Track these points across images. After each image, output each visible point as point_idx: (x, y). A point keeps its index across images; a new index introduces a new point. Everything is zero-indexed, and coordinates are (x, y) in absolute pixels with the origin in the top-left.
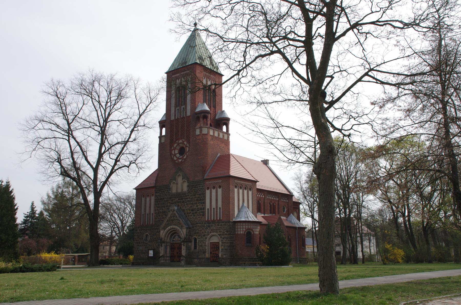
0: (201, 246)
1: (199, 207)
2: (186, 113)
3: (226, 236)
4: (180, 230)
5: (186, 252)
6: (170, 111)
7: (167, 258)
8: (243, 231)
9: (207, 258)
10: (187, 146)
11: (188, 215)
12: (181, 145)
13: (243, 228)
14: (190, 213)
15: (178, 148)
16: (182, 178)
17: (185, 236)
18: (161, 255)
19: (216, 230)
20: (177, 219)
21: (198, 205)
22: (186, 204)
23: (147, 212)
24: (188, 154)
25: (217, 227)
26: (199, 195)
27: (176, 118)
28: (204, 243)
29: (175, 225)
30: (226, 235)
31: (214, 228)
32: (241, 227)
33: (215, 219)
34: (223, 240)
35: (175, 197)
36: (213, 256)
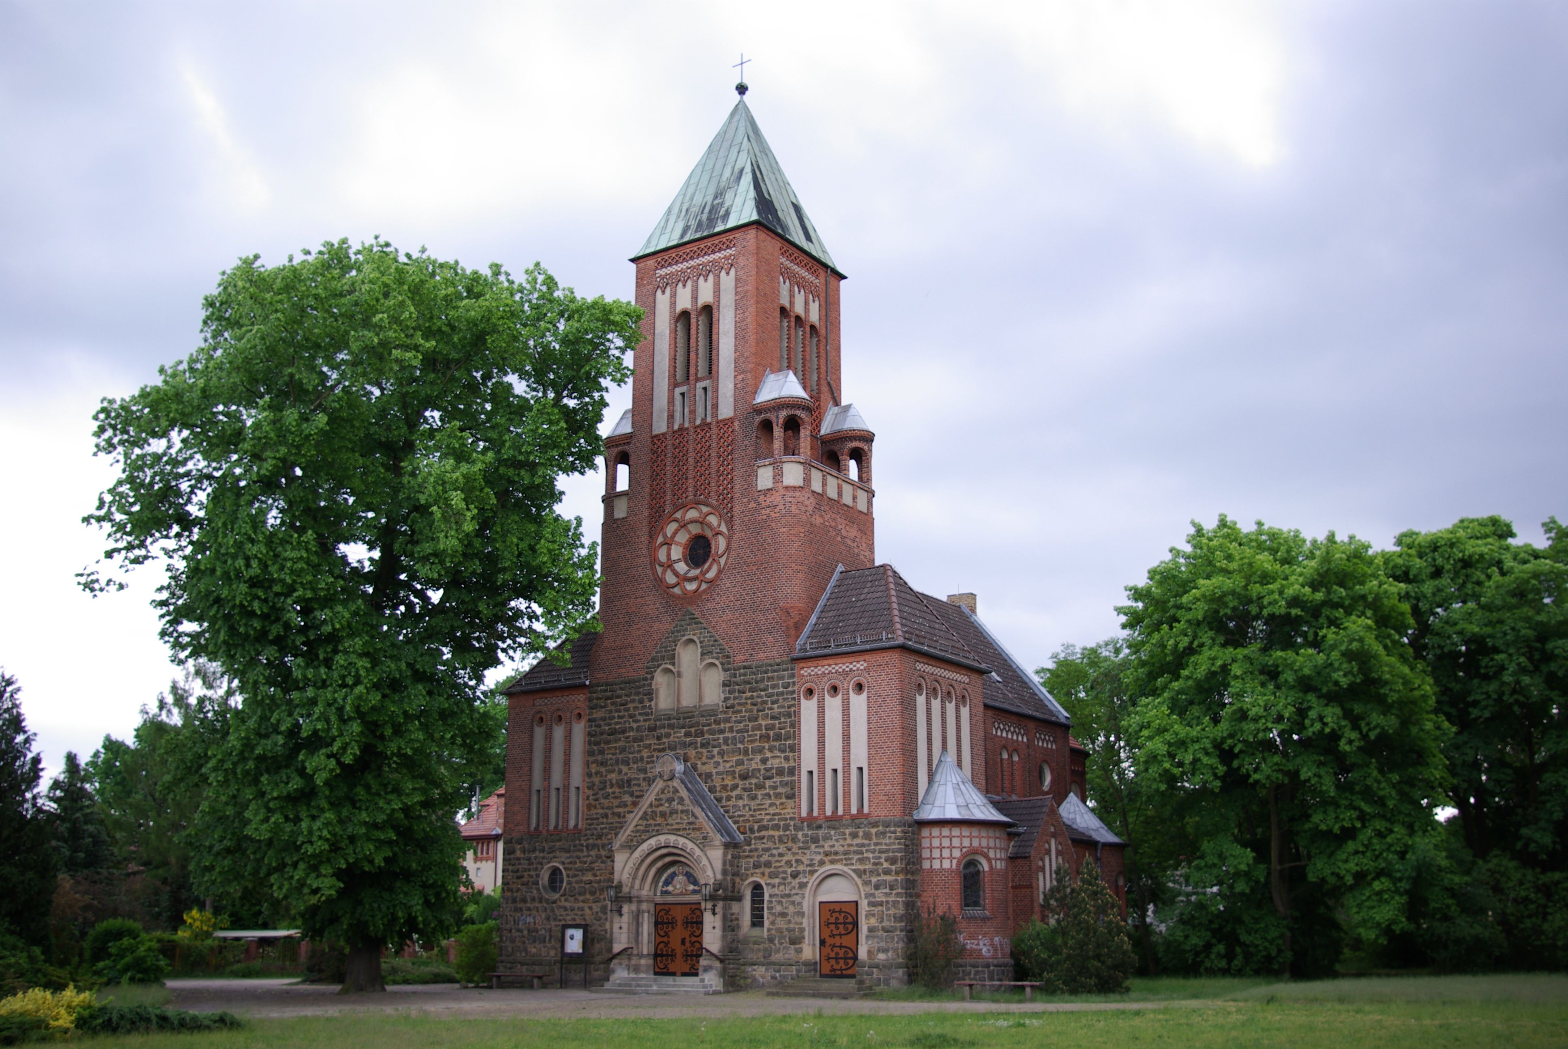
0: (783, 915)
1: (774, 763)
2: (715, 406)
3: (888, 878)
4: (698, 852)
5: (724, 937)
6: (652, 400)
7: (643, 962)
8: (951, 858)
9: (806, 964)
10: (719, 533)
11: (724, 795)
12: (695, 529)
13: (951, 848)
14: (735, 787)
15: (683, 538)
16: (702, 654)
17: (719, 876)
18: (617, 948)
19: (846, 853)
20: (682, 812)
21: (768, 755)
22: (716, 751)
23: (834, 759)
24: (723, 561)
25: (849, 841)
26: (773, 718)
27: (676, 427)
28: (793, 903)
29: (675, 832)
30: (887, 872)
31: (838, 848)
32: (946, 843)
33: (840, 812)
34: (873, 895)
35: (671, 726)
36: (833, 955)
